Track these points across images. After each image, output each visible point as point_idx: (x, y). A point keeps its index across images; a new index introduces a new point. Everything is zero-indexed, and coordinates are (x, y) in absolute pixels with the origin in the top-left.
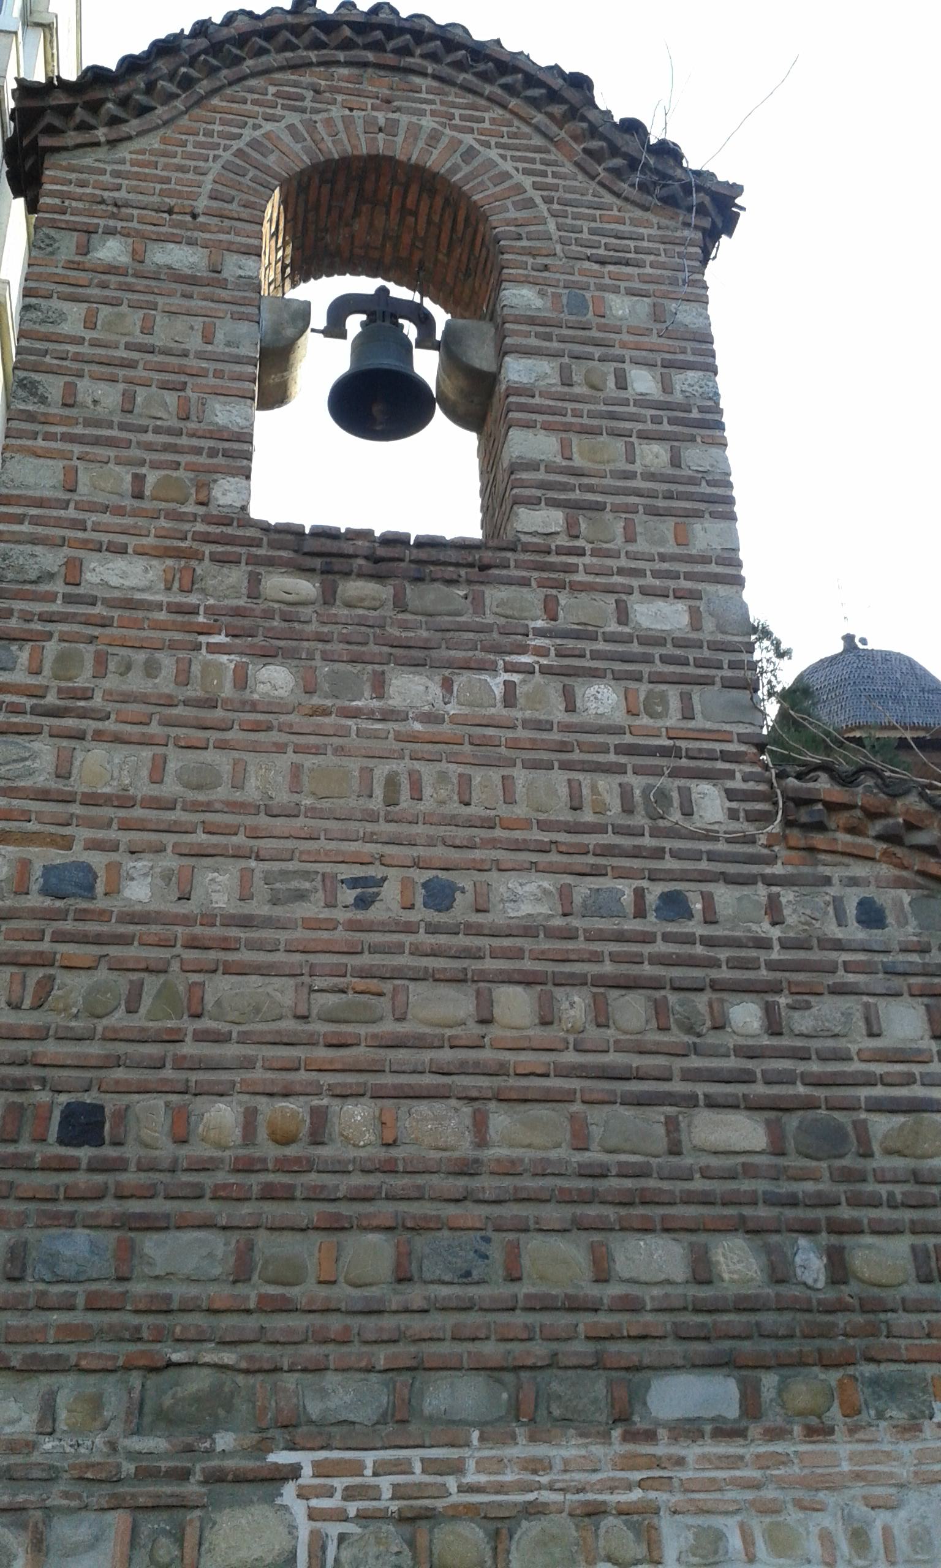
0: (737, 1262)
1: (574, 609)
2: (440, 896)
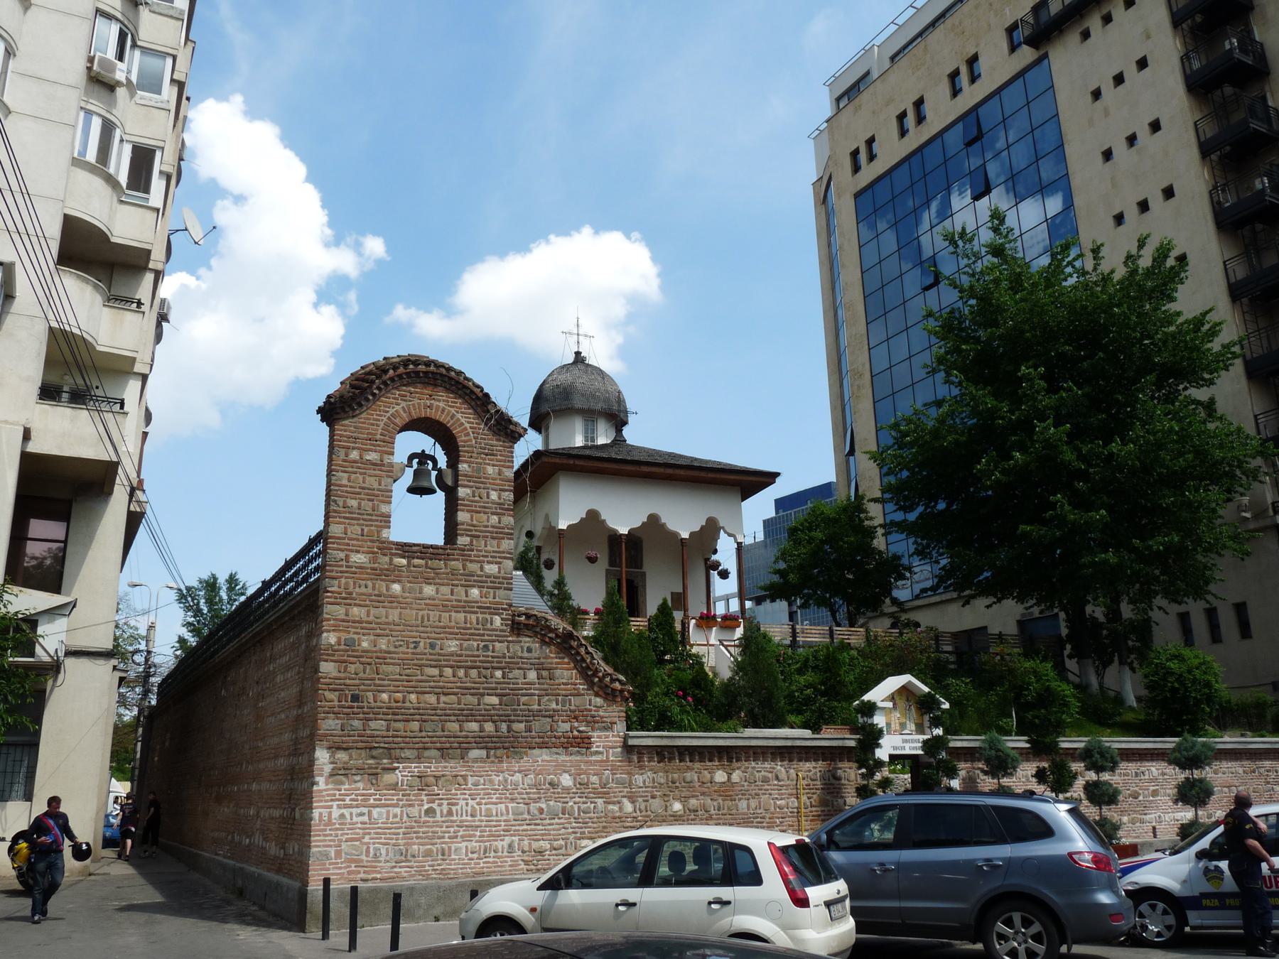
0: (489, 727)
1: (473, 567)
2: (432, 646)
